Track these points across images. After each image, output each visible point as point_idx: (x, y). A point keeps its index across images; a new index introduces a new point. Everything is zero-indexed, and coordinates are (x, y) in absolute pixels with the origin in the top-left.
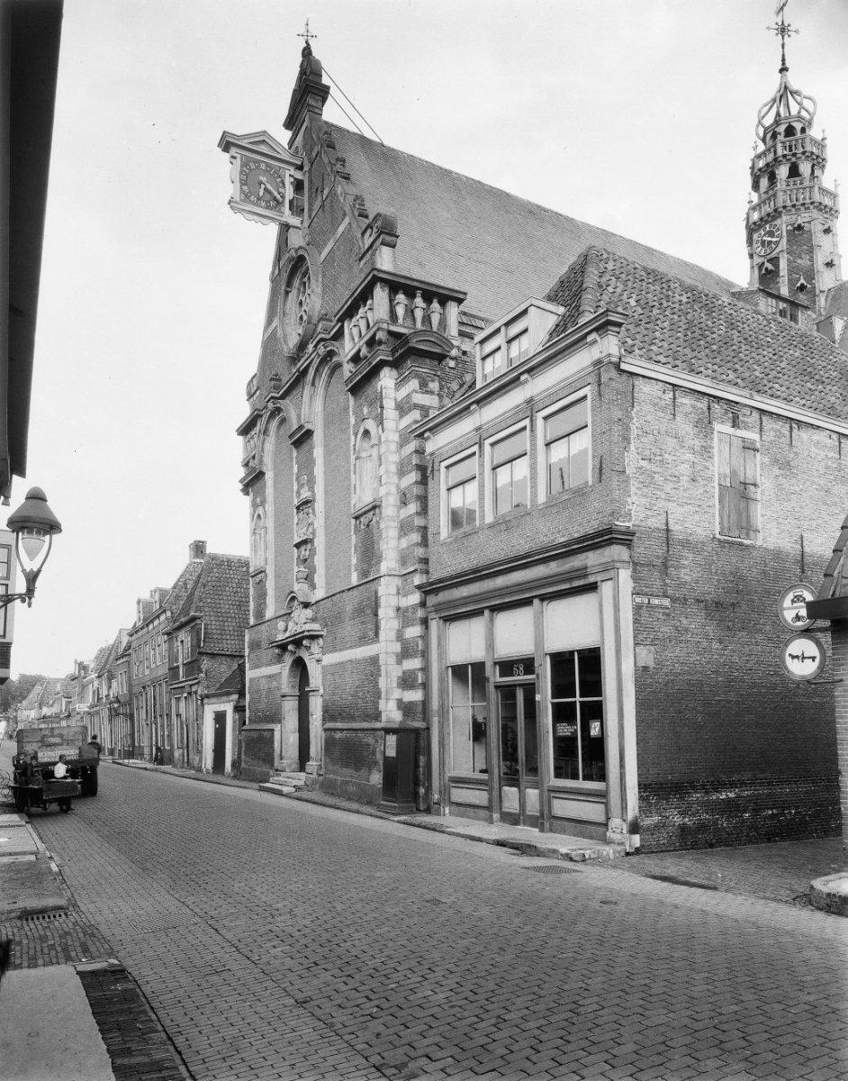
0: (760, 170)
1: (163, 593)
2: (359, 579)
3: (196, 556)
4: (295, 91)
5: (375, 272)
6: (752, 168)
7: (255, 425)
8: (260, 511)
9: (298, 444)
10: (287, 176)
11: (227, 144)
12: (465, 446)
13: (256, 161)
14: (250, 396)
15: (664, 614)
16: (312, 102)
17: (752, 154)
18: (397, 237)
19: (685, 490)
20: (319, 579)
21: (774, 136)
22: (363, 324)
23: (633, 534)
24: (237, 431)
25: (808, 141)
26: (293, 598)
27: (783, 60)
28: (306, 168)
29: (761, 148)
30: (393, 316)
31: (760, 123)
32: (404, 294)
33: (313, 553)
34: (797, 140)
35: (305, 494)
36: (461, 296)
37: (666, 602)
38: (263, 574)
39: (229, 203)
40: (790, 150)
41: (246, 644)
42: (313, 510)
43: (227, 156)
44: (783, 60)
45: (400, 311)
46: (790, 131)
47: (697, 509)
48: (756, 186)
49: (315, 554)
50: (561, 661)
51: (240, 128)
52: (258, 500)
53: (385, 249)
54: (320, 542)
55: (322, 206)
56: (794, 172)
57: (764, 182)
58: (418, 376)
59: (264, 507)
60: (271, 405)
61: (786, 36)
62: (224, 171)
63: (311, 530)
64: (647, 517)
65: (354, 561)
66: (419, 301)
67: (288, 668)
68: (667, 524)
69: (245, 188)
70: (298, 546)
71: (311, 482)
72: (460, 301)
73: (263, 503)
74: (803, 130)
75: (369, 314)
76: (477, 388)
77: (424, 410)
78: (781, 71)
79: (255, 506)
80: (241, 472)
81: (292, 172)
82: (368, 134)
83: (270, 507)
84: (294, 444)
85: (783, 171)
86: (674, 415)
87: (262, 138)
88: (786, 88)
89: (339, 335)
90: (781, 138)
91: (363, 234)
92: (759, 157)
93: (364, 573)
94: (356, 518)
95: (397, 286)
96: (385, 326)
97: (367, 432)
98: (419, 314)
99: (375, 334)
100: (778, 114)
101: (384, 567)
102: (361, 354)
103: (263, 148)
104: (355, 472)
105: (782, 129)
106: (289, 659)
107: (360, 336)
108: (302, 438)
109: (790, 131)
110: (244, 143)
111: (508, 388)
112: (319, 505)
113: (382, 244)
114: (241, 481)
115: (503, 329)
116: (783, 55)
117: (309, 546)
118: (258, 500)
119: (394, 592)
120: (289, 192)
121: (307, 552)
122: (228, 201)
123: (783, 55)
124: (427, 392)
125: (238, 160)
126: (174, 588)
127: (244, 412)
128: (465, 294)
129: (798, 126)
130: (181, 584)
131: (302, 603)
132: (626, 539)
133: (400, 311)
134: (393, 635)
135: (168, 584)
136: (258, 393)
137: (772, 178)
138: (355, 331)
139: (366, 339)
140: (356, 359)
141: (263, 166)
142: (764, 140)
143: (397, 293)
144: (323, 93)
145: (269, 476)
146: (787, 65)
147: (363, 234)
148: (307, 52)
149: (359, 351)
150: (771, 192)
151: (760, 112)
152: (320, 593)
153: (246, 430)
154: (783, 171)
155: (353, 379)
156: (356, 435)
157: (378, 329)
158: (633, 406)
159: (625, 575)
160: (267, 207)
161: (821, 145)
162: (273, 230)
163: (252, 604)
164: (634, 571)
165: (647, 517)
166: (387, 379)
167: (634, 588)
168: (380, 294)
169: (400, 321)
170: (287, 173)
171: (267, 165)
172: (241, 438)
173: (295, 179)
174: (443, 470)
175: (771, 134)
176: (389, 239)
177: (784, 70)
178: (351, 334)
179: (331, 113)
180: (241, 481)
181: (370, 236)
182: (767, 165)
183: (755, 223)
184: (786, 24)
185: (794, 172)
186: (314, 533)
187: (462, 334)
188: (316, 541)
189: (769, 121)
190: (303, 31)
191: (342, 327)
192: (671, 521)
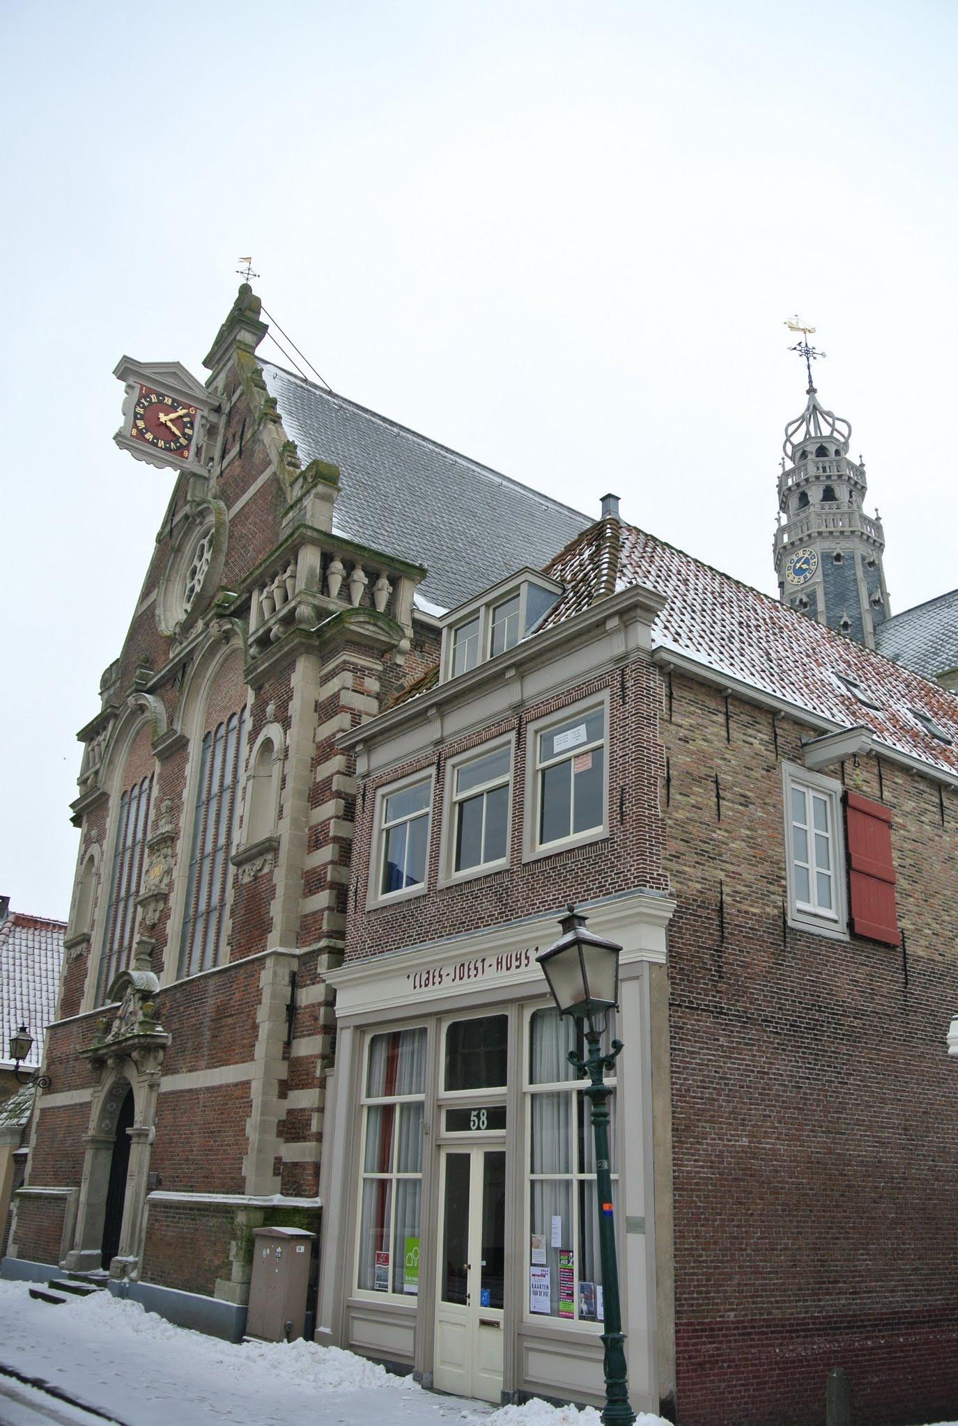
0: (789, 489)
6: (779, 486)
7: (105, 728)
9: (164, 756)
11: (127, 369)
13: (158, 395)
17: (780, 472)
18: (339, 490)
20: (170, 955)
21: (804, 455)
22: (278, 595)
25: (843, 465)
27: (811, 382)
29: (789, 465)
31: (788, 440)
33: (165, 916)
34: (831, 462)
35: (165, 828)
38: (84, 945)
40: (824, 471)
43: (123, 384)
44: (811, 382)
46: (822, 451)
48: (784, 507)
49: (168, 917)
51: (145, 355)
52: (94, 833)
56: (829, 495)
57: (794, 502)
59: (101, 846)
60: (131, 701)
61: (811, 358)
63: (166, 881)
66: (359, 576)
69: (141, 424)
71: (174, 810)
73: (100, 840)
74: (837, 453)
75: (289, 583)
77: (356, 717)
78: (808, 392)
79: (87, 841)
80: (75, 793)
81: (206, 413)
82: (312, 378)
83: (109, 843)
84: (160, 755)
85: (815, 494)
87: (175, 370)
88: (815, 408)
89: (242, 611)
90: (811, 457)
92: (786, 474)
94: (238, 864)
95: (331, 549)
97: (268, 743)
99: (294, 609)
100: (808, 432)
101: (274, 943)
102: (272, 634)
103: (171, 382)
104: (244, 799)
105: (812, 448)
107: (274, 609)
108: (174, 749)
109: (822, 451)
110: (147, 372)
112: (182, 845)
114: (72, 806)
116: (810, 376)
117: (161, 906)
118: (94, 833)
121: (157, 914)
122: (113, 434)
123: (810, 376)
125: (137, 390)
127: (93, 707)
129: (832, 449)
131: (139, 991)
136: (118, 684)
137: (804, 499)
138: (266, 605)
139: (281, 615)
140: (264, 641)
142: (792, 458)
143: (332, 560)
146: (815, 385)
150: (802, 515)
151: (786, 430)
153: (87, 735)
154: (815, 494)
155: (255, 669)
156: (252, 741)
157: (300, 603)
161: (860, 470)
162: (170, 477)
166: (302, 675)
168: (309, 558)
170: (199, 413)
172: (83, 744)
175: (800, 454)
177: (811, 391)
180: (72, 806)
181: (302, 487)
182: (798, 485)
183: (784, 547)
184: (810, 346)
185: (829, 495)
186: (170, 885)
188: (172, 896)
189: (798, 438)
191: (250, 598)
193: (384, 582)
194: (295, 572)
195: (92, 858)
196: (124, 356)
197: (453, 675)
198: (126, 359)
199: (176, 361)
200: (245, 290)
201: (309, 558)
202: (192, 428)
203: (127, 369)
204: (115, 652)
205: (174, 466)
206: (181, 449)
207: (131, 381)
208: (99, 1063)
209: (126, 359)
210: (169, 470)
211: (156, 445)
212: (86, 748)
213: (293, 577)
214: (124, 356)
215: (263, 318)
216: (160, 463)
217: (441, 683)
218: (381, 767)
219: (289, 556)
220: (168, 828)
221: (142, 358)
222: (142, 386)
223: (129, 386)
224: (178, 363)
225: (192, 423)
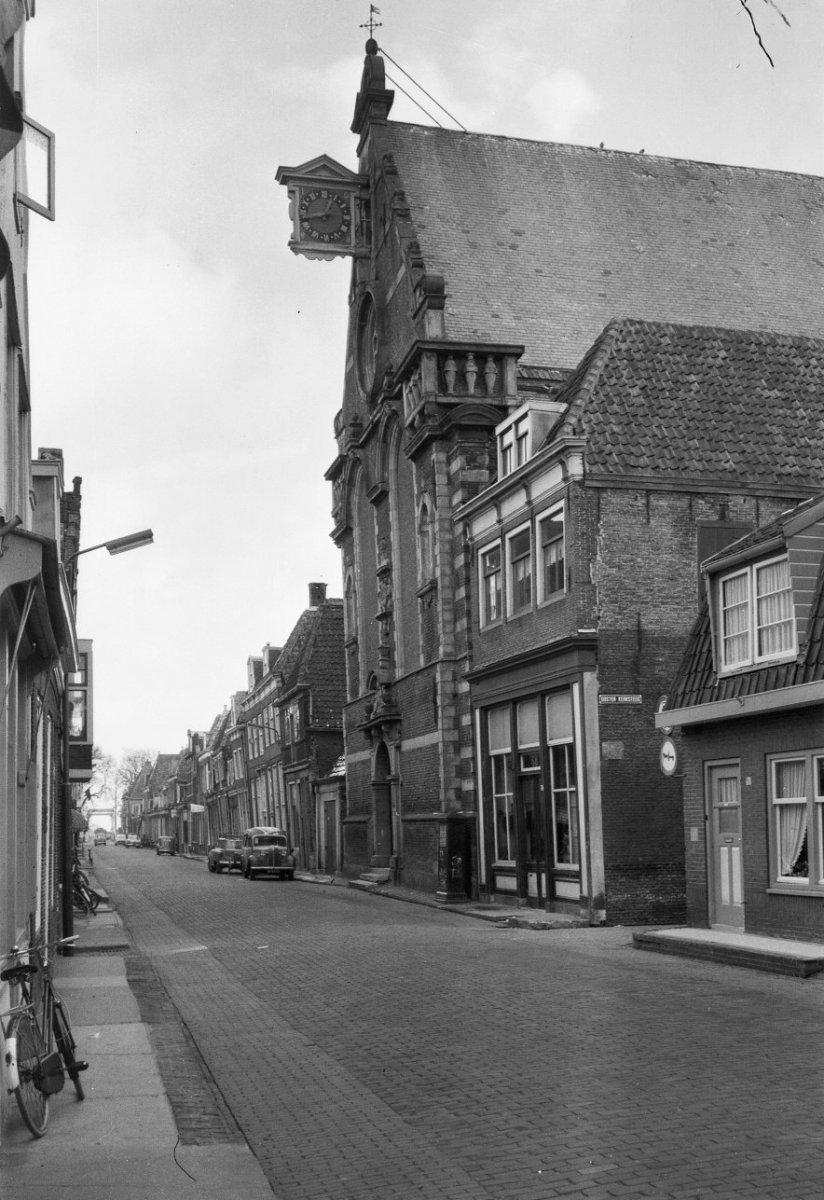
1: (273, 653)
2: (426, 662)
3: (313, 603)
4: (358, 94)
5: (418, 345)
8: (350, 572)
10: (352, 199)
11: (285, 176)
12: (490, 538)
14: (338, 433)
15: (634, 710)
16: (374, 112)
19: (660, 591)
23: (595, 640)
24: (325, 475)
26: (375, 678)
28: (372, 190)
30: (442, 385)
32: (454, 358)
36: (519, 350)
37: (638, 699)
39: (290, 244)
41: (344, 726)
42: (392, 580)
45: (451, 378)
47: (676, 607)
50: (558, 749)
51: (294, 162)
53: (431, 313)
54: (396, 616)
55: (385, 241)
58: (463, 451)
62: (278, 209)
64: (616, 620)
65: (421, 642)
67: (375, 754)
68: (639, 625)
69: (306, 224)
70: (379, 618)
72: (519, 356)
76: (500, 480)
80: (331, 525)
82: (448, 124)
84: (373, 502)
86: (648, 519)
87: (325, 163)
91: (415, 291)
93: (429, 657)
94: (421, 596)
96: (432, 399)
98: (472, 379)
103: (324, 175)
106: (377, 745)
111: (514, 489)
113: (429, 308)
114: (332, 535)
115: (513, 426)
119: (450, 678)
120: (355, 216)
122: (287, 242)
124: (475, 467)
126: (286, 646)
128: (522, 347)
130: (297, 639)
131: (382, 684)
132: (588, 645)
133: (451, 378)
134: (450, 723)
135: (280, 642)
139: (419, 408)
141: (324, 194)
144: (388, 98)
145: (356, 532)
147: (415, 291)
148: (372, 47)
149: (414, 419)
152: (399, 673)
153: (333, 474)
157: (426, 403)
158: (599, 519)
159: (589, 677)
160: (331, 241)
163: (348, 678)
164: (601, 673)
165: (616, 620)
166: (436, 456)
167: (600, 688)
168: (428, 365)
169: (451, 390)
171: (329, 191)
172: (331, 482)
173: (361, 200)
174: (480, 557)
176: (436, 302)
178: (408, 398)
179: (396, 114)
186: (392, 606)
187: (520, 388)
190: (365, 20)
192: (643, 621)
193: (491, 366)
194: (420, 374)
195: (349, 577)
196: (280, 168)
197: (505, 472)
198: (281, 169)
199: (322, 154)
200: (372, 47)
201: (428, 365)
202: (349, 213)
203: (285, 176)
204: (339, 405)
205: (343, 255)
206: (344, 236)
207: (291, 183)
208: (369, 736)
209: (281, 169)
210: (338, 258)
211: (322, 241)
212: (334, 484)
213: (420, 378)
214: (280, 168)
215: (389, 86)
216: (330, 255)
217: (500, 480)
218: (480, 533)
219: (412, 365)
220: (384, 563)
221: (294, 163)
222: (300, 187)
223: (291, 192)
224: (325, 157)
225: (348, 208)
